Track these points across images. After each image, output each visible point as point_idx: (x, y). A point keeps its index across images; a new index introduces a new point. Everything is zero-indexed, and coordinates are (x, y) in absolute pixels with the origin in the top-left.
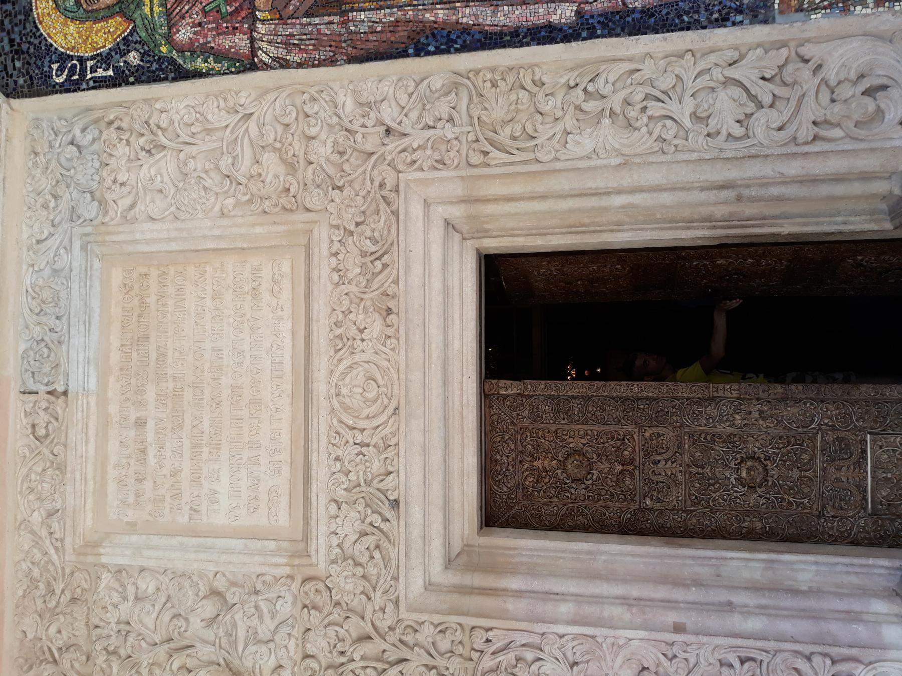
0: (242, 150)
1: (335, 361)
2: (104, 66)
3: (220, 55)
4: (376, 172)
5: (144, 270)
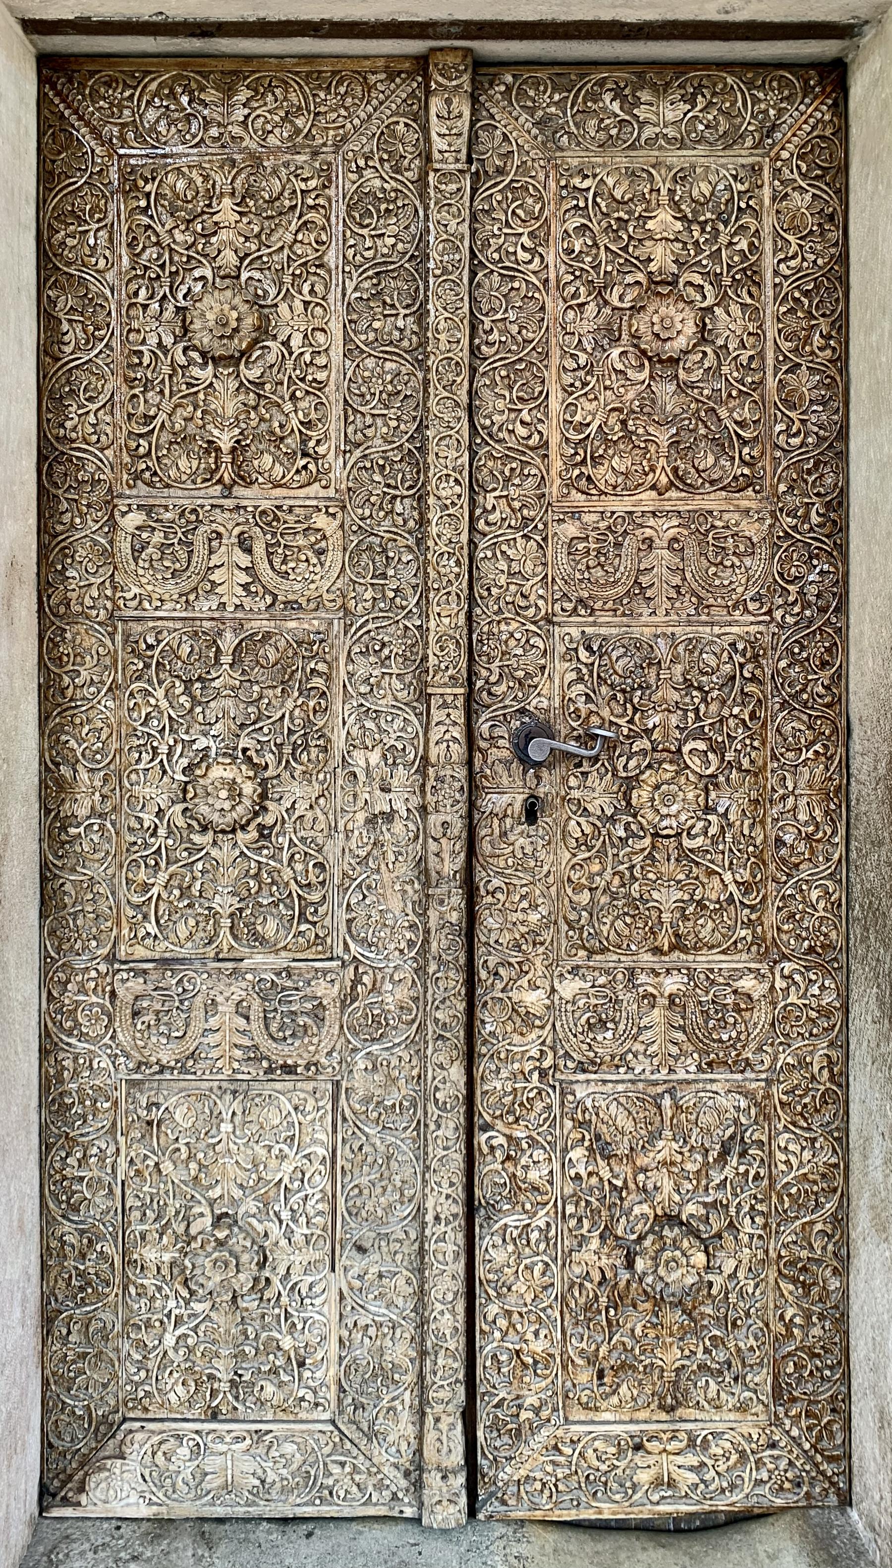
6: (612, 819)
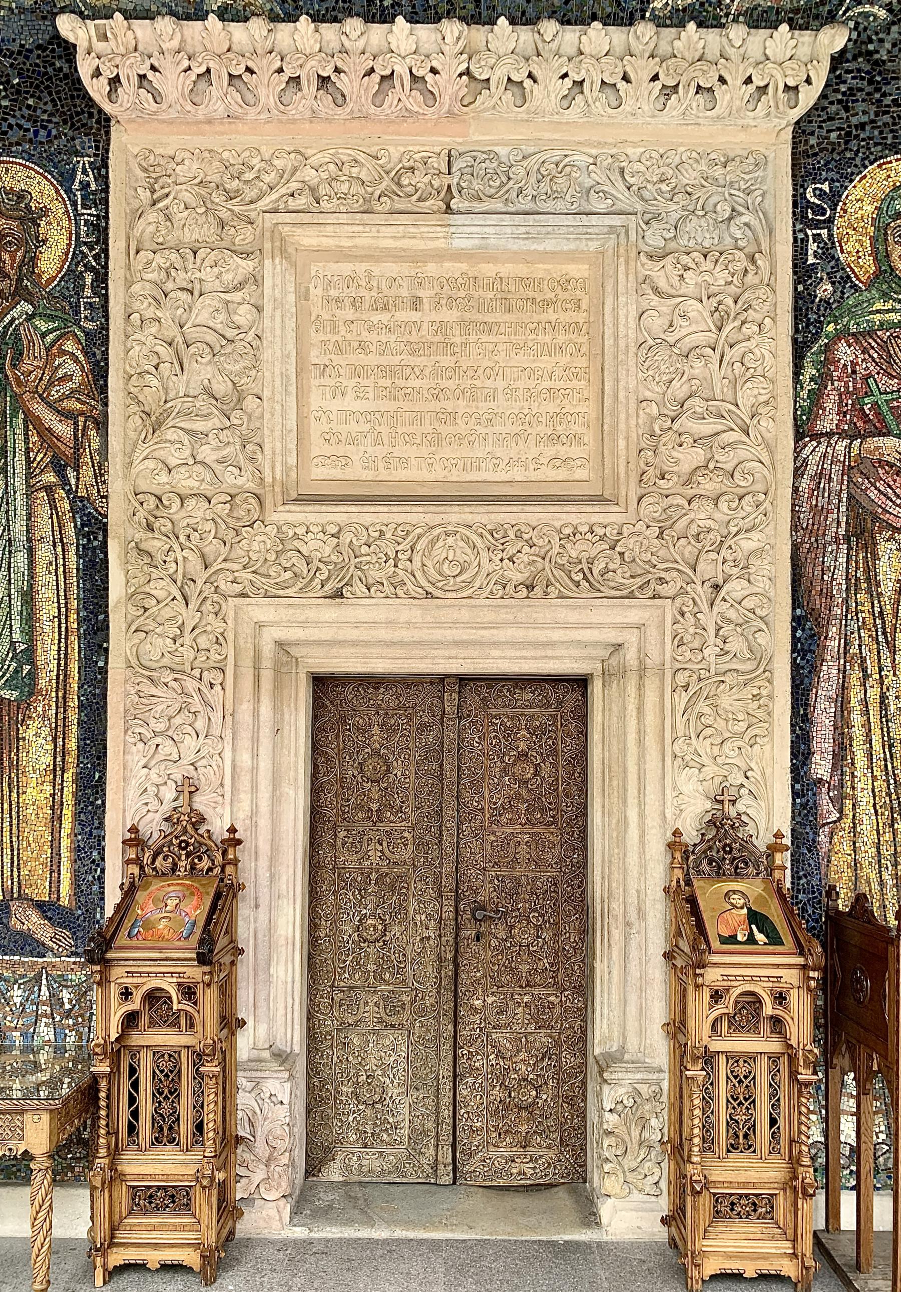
0: (710, 423)
1: (480, 530)
2: (820, 251)
3: (816, 397)
4: (675, 574)
5: (584, 306)
6: (506, 940)
